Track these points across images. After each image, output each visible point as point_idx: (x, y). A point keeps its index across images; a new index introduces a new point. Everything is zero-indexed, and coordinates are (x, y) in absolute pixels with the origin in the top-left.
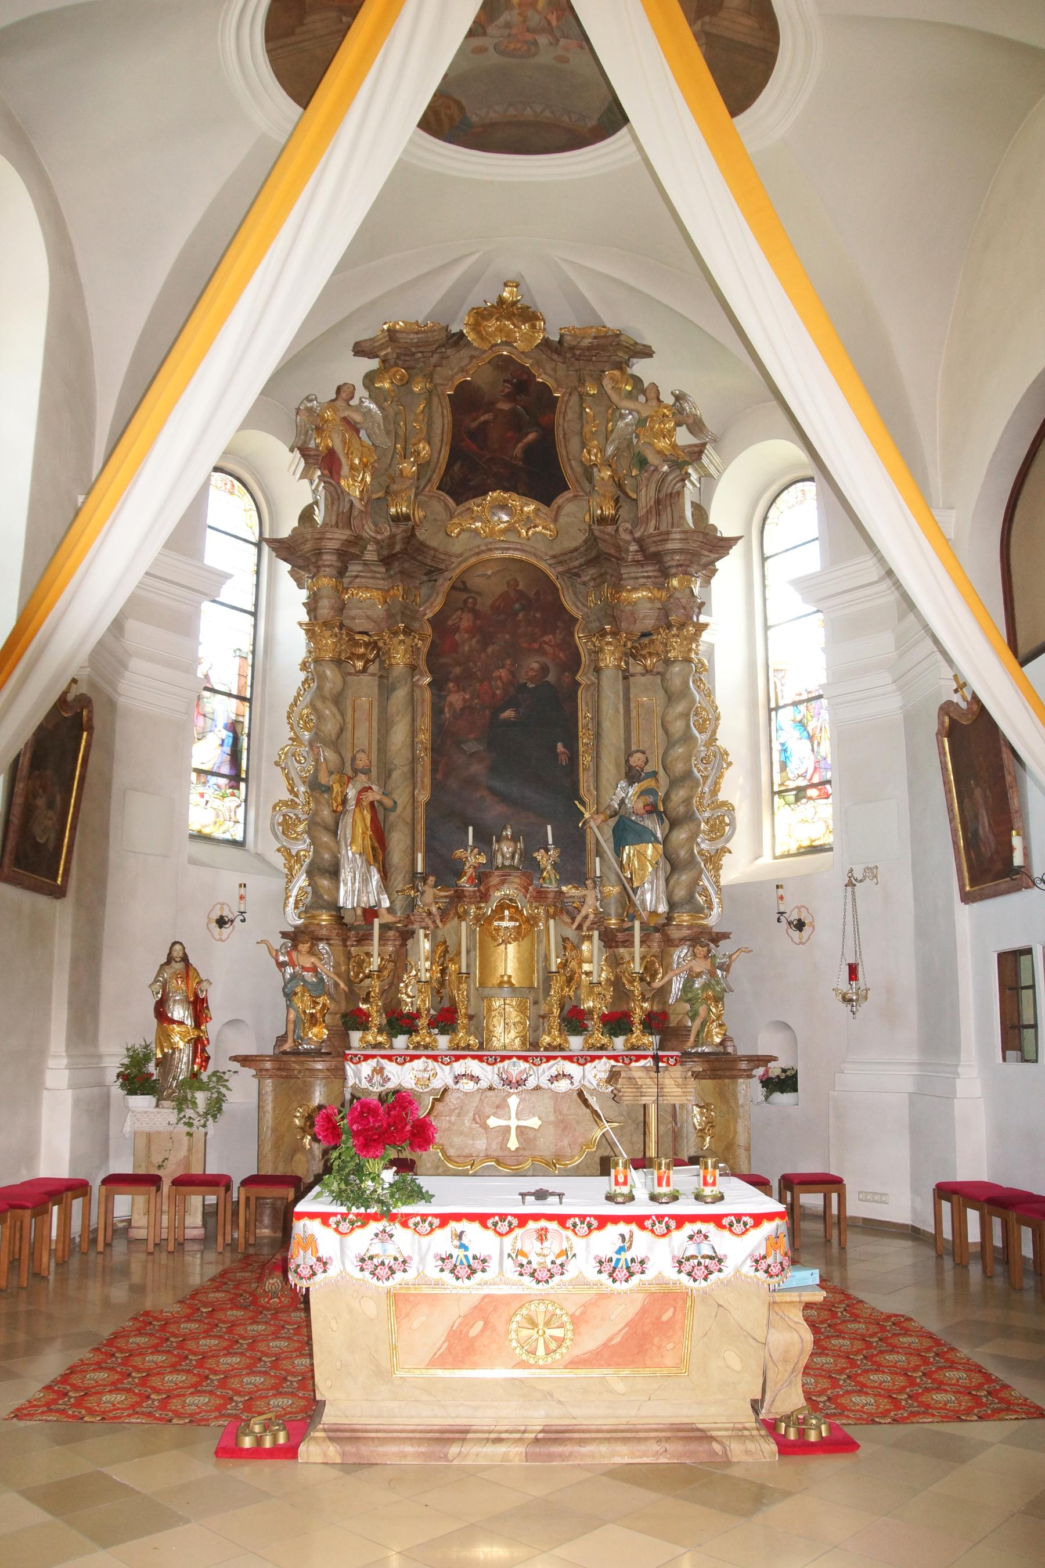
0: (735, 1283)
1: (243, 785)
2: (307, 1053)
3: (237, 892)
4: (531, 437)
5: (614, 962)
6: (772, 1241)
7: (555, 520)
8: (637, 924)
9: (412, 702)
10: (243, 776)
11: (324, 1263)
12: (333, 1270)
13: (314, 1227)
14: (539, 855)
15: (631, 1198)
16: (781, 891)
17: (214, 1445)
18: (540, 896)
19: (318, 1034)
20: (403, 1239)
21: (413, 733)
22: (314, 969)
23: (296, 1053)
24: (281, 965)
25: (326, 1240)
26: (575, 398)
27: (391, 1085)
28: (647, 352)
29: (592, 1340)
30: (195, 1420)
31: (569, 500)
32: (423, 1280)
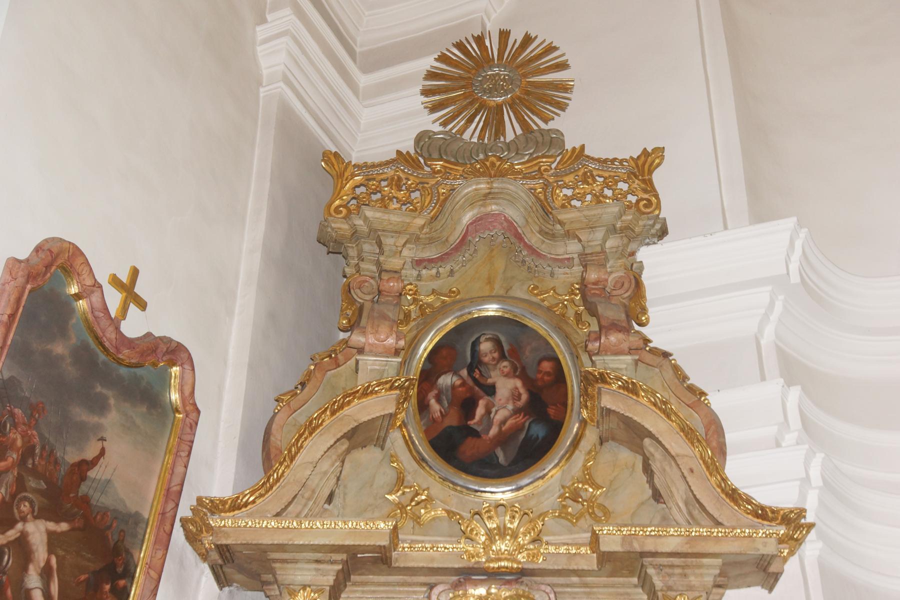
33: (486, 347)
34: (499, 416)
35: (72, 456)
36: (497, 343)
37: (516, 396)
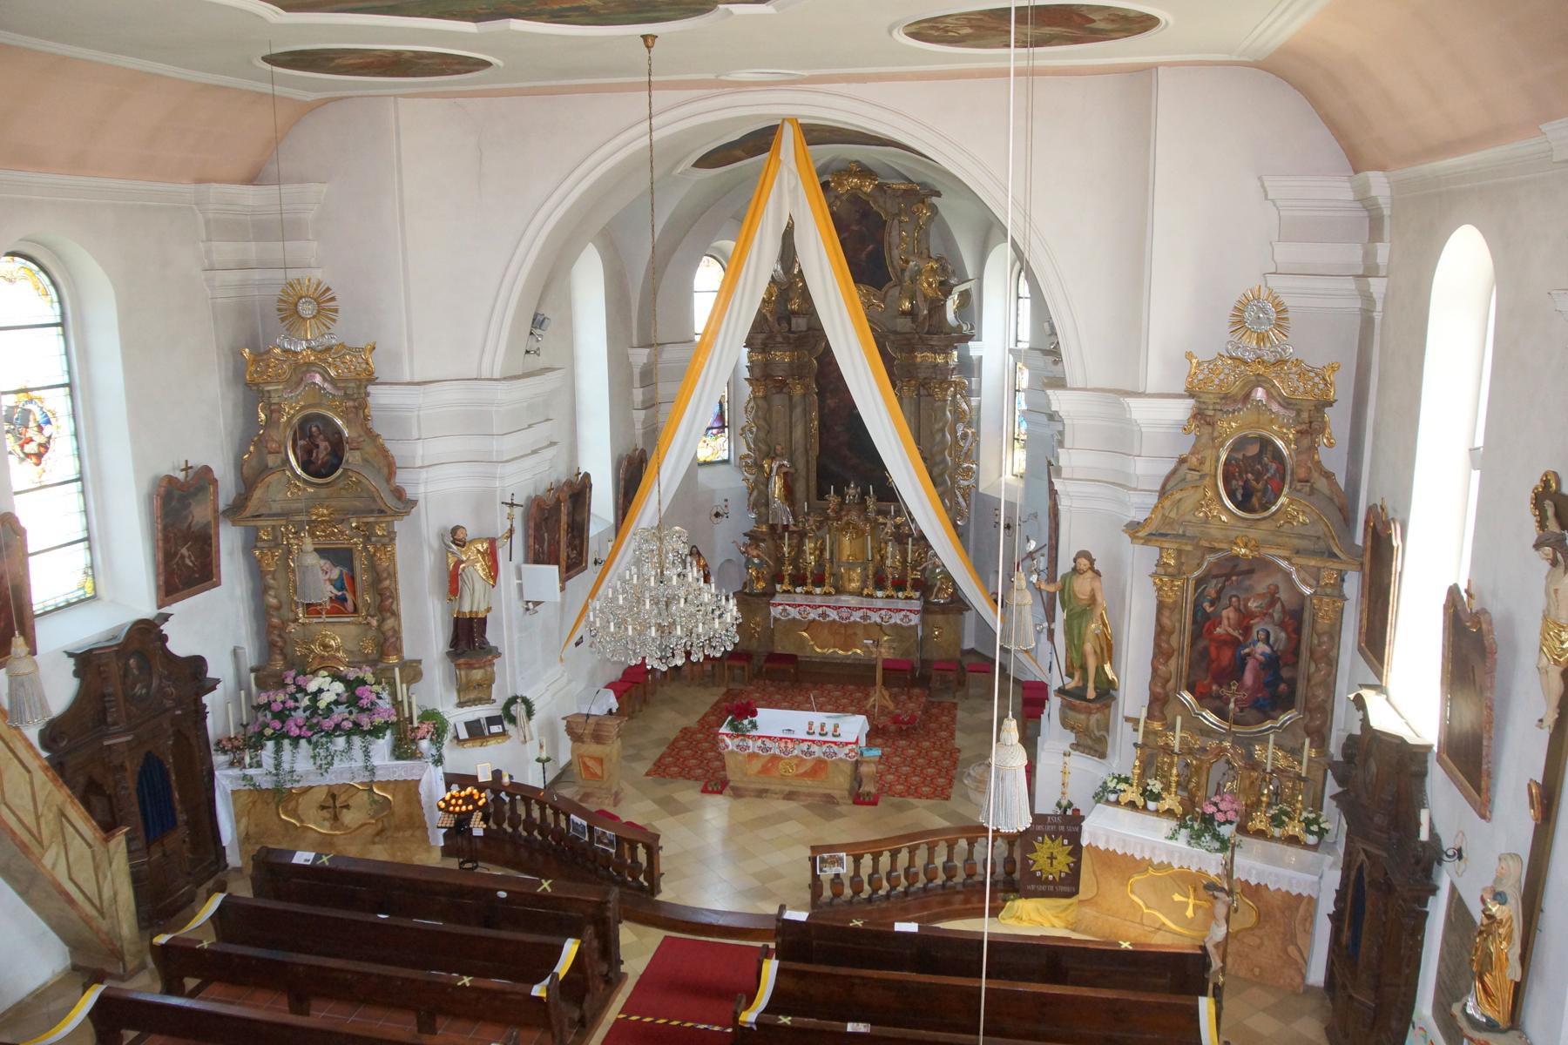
0: (841, 759)
1: (726, 430)
2: (757, 595)
4: (871, 247)
5: (904, 554)
6: (851, 750)
8: (910, 540)
9: (806, 412)
11: (727, 746)
12: (730, 748)
13: (725, 737)
14: (867, 497)
17: (699, 788)
18: (867, 520)
19: (760, 586)
20: (750, 743)
21: (807, 434)
22: (758, 556)
23: (750, 595)
25: (728, 741)
26: (896, 221)
28: (938, 194)
29: (802, 770)
30: (697, 779)
31: (891, 288)
32: (754, 753)
33: (314, 429)
34: (321, 456)
35: (186, 525)
36: (318, 427)
37: (326, 449)
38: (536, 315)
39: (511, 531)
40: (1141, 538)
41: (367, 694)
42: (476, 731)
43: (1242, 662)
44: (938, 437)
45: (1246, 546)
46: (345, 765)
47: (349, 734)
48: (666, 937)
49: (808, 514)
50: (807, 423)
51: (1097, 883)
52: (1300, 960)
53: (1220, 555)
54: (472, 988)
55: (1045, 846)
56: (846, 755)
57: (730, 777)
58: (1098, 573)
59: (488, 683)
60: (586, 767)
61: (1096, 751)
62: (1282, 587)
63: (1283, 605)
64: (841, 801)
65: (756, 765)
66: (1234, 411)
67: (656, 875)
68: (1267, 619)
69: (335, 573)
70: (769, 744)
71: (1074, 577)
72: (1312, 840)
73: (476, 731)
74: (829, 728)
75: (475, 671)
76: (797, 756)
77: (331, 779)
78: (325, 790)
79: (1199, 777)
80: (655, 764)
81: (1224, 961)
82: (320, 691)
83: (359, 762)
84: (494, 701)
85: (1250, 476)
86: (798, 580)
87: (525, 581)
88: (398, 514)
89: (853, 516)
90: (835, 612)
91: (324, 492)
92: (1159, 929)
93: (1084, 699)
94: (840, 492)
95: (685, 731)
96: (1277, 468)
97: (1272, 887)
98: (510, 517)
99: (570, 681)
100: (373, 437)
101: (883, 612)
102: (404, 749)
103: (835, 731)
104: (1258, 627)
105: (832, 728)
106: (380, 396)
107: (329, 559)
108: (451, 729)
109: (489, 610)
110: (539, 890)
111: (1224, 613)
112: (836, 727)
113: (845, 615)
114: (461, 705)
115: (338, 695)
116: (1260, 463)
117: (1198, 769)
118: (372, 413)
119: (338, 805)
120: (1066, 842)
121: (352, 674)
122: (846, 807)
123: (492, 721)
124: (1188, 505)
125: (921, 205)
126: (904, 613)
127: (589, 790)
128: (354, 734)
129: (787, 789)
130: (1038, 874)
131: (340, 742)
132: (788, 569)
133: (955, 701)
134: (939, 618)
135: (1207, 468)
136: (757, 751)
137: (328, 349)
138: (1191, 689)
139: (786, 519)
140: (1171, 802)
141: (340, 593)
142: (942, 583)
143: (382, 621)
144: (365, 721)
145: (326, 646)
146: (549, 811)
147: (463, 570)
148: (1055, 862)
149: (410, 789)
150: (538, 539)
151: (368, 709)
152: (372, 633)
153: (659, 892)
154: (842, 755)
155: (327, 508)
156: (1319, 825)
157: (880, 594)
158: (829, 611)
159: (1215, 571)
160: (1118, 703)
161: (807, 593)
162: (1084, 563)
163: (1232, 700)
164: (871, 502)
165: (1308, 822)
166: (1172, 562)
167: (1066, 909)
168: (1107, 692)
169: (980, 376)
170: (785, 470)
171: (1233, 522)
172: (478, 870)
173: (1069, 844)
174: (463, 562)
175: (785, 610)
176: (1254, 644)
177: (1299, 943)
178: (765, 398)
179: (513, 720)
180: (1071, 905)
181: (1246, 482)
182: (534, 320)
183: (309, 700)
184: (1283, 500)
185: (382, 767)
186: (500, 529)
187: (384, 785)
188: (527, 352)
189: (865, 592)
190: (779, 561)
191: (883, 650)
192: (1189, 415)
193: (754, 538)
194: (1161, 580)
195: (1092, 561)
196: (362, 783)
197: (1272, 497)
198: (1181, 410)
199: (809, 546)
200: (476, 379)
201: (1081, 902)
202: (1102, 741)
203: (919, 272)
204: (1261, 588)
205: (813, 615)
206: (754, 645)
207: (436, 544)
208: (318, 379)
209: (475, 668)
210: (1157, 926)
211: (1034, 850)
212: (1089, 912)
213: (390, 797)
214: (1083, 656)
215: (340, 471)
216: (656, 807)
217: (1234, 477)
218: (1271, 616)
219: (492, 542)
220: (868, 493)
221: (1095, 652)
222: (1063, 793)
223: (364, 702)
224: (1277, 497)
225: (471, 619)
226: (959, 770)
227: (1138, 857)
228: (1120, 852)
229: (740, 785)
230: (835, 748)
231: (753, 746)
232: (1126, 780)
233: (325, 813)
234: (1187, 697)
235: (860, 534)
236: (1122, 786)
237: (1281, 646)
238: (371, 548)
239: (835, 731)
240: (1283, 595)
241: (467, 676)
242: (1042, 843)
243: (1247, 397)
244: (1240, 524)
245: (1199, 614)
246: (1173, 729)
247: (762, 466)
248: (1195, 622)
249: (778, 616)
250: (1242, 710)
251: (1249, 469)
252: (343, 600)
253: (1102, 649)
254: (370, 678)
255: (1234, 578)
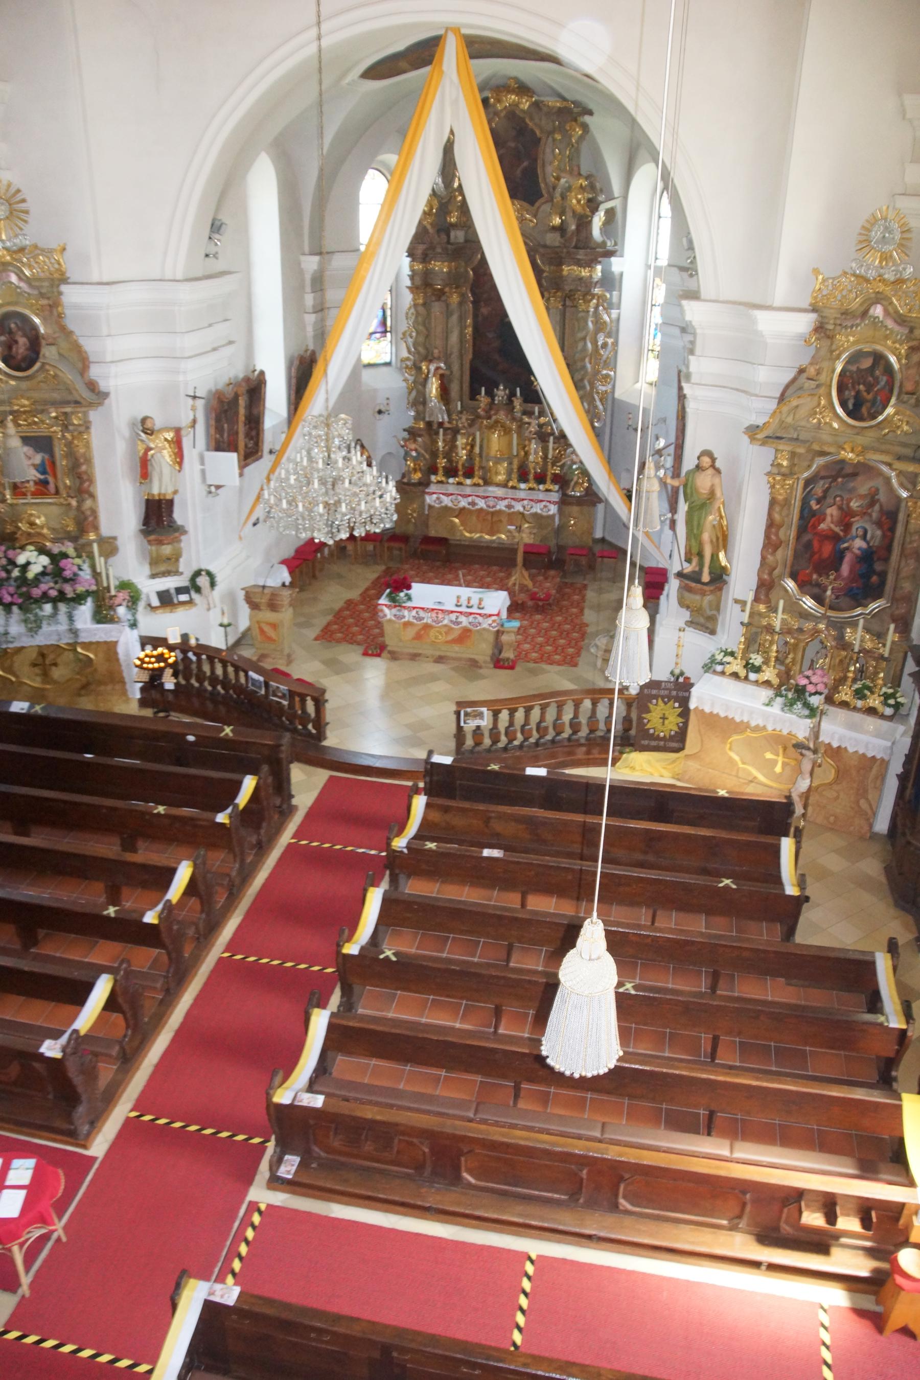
0: (484, 629)
1: (389, 335)
2: (414, 485)
3: (385, 402)
5: (545, 450)
6: (494, 621)
7: (535, 216)
8: (551, 439)
9: (462, 319)
10: (388, 329)
11: (385, 615)
15: (460, 606)
16: (630, 416)
18: (514, 419)
19: (417, 476)
20: (406, 613)
21: (462, 335)
22: (416, 450)
23: (409, 484)
24: (402, 446)
25: (386, 610)
27: (443, 504)
28: (590, 113)
29: (450, 638)
30: (359, 644)
33: (13, 326)
36: (16, 323)
37: (25, 345)
38: (214, 220)
39: (194, 421)
40: (759, 440)
41: (69, 566)
42: (166, 600)
43: (839, 557)
44: (580, 345)
45: (852, 451)
46: (53, 628)
47: (54, 601)
48: (331, 777)
49: (461, 412)
50: (463, 328)
51: (702, 741)
52: (869, 812)
53: (828, 459)
54: (166, 816)
55: (659, 708)
56: (490, 625)
57: (387, 642)
58: (718, 471)
59: (176, 557)
60: (262, 631)
61: (707, 628)
62: (881, 491)
63: (881, 506)
64: (483, 665)
65: (411, 633)
66: (852, 327)
67: (322, 724)
68: (866, 518)
69: (38, 458)
70: (422, 614)
71: (697, 473)
72: (889, 711)
73: (166, 600)
74: (474, 602)
75: (164, 547)
76: (446, 626)
77: (41, 639)
78: (37, 649)
79: (795, 654)
80: (322, 631)
81: (805, 807)
82: (28, 563)
83: (63, 626)
84: (182, 573)
85: (861, 387)
86: (451, 472)
87: (207, 467)
88: (91, 405)
89: (502, 416)
90: (483, 501)
91: (24, 385)
92: (751, 781)
93: (698, 581)
94: (490, 394)
95: (349, 603)
96: (887, 382)
97: (851, 750)
98: (194, 409)
99: (248, 557)
100: (67, 333)
101: (526, 502)
102: (103, 615)
103: (480, 604)
104: (858, 524)
105: (477, 602)
106: (71, 295)
107: (31, 446)
108: (143, 597)
109: (176, 492)
110: (222, 735)
111: (829, 511)
112: (481, 600)
113: (491, 504)
114: (153, 576)
115: (45, 567)
116: (872, 375)
117: (796, 646)
118: (67, 312)
119: (47, 662)
120: (677, 705)
121: (56, 549)
122: (488, 671)
123: (180, 591)
124: (803, 412)
125: (574, 123)
126: (544, 503)
127: (265, 652)
128: (60, 601)
129: (438, 653)
130: (651, 731)
131: (48, 608)
132: (442, 462)
133: (585, 582)
134: (575, 509)
135: (823, 378)
136: (411, 620)
137: (22, 250)
138: (794, 576)
139: (442, 417)
140: (769, 674)
141: (42, 477)
142: (579, 478)
143: (80, 502)
144: (68, 590)
145: (32, 524)
146: (230, 669)
147: (152, 456)
148: (666, 722)
149: (110, 648)
150: (219, 429)
151: (71, 579)
152: (73, 513)
153: (325, 738)
154: (485, 626)
155: (28, 399)
156: (896, 698)
157: (523, 486)
158: (477, 500)
159: (823, 474)
160: (729, 588)
161: (459, 484)
162: (706, 461)
163: (830, 588)
164: (517, 403)
165: (887, 697)
166: (785, 463)
167: (674, 761)
168: (719, 577)
169: (620, 291)
170: (441, 372)
171: (843, 429)
172: (170, 718)
173: (680, 707)
174: (151, 449)
175: (438, 498)
176: (853, 539)
177: (870, 797)
178: (424, 304)
179: (198, 590)
180: (678, 758)
181: (858, 393)
182: (212, 225)
183: (19, 571)
184: (890, 410)
185: (86, 630)
186: (184, 419)
187: (87, 646)
188: (207, 256)
189: (510, 484)
190: (434, 454)
191: (524, 535)
192: (811, 329)
193: (412, 433)
194: (774, 479)
195: (714, 460)
196: (68, 644)
197: (880, 407)
198: (804, 323)
199: (461, 441)
200: (160, 280)
201: (687, 756)
202: (713, 619)
203: (569, 189)
204: (863, 490)
205: (463, 503)
206: (410, 529)
207: (126, 432)
208: (14, 278)
209: (163, 544)
210: (750, 779)
211: (649, 711)
212: (693, 765)
213: (92, 656)
214: (701, 545)
215: (37, 366)
216: (322, 667)
217: (847, 388)
218: (870, 515)
219: (178, 431)
220: (514, 395)
221: (711, 541)
222: (677, 664)
223: (68, 574)
224: (885, 407)
225: (160, 501)
226: (586, 641)
227: (738, 719)
228: (722, 715)
229: (395, 649)
230: (480, 619)
231: (408, 616)
232: (732, 654)
233: (37, 670)
234: (790, 584)
235: (507, 431)
236: (729, 659)
237: (876, 542)
238: (68, 435)
239: (480, 604)
240: (882, 497)
241: (157, 550)
242: (656, 705)
243: (865, 313)
244: (849, 431)
245: (806, 511)
246: (776, 611)
247: (420, 368)
248: (801, 517)
249: (433, 504)
250: (837, 597)
251: (862, 381)
252: (45, 483)
253: (718, 539)
254: (71, 551)
255: (840, 480)
